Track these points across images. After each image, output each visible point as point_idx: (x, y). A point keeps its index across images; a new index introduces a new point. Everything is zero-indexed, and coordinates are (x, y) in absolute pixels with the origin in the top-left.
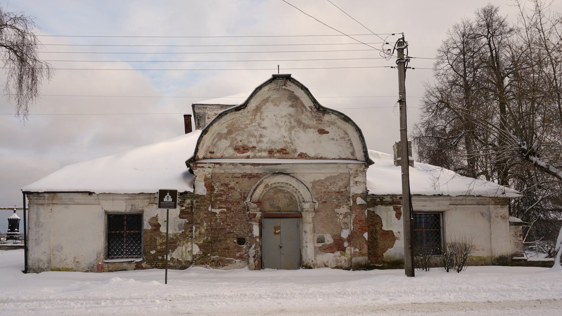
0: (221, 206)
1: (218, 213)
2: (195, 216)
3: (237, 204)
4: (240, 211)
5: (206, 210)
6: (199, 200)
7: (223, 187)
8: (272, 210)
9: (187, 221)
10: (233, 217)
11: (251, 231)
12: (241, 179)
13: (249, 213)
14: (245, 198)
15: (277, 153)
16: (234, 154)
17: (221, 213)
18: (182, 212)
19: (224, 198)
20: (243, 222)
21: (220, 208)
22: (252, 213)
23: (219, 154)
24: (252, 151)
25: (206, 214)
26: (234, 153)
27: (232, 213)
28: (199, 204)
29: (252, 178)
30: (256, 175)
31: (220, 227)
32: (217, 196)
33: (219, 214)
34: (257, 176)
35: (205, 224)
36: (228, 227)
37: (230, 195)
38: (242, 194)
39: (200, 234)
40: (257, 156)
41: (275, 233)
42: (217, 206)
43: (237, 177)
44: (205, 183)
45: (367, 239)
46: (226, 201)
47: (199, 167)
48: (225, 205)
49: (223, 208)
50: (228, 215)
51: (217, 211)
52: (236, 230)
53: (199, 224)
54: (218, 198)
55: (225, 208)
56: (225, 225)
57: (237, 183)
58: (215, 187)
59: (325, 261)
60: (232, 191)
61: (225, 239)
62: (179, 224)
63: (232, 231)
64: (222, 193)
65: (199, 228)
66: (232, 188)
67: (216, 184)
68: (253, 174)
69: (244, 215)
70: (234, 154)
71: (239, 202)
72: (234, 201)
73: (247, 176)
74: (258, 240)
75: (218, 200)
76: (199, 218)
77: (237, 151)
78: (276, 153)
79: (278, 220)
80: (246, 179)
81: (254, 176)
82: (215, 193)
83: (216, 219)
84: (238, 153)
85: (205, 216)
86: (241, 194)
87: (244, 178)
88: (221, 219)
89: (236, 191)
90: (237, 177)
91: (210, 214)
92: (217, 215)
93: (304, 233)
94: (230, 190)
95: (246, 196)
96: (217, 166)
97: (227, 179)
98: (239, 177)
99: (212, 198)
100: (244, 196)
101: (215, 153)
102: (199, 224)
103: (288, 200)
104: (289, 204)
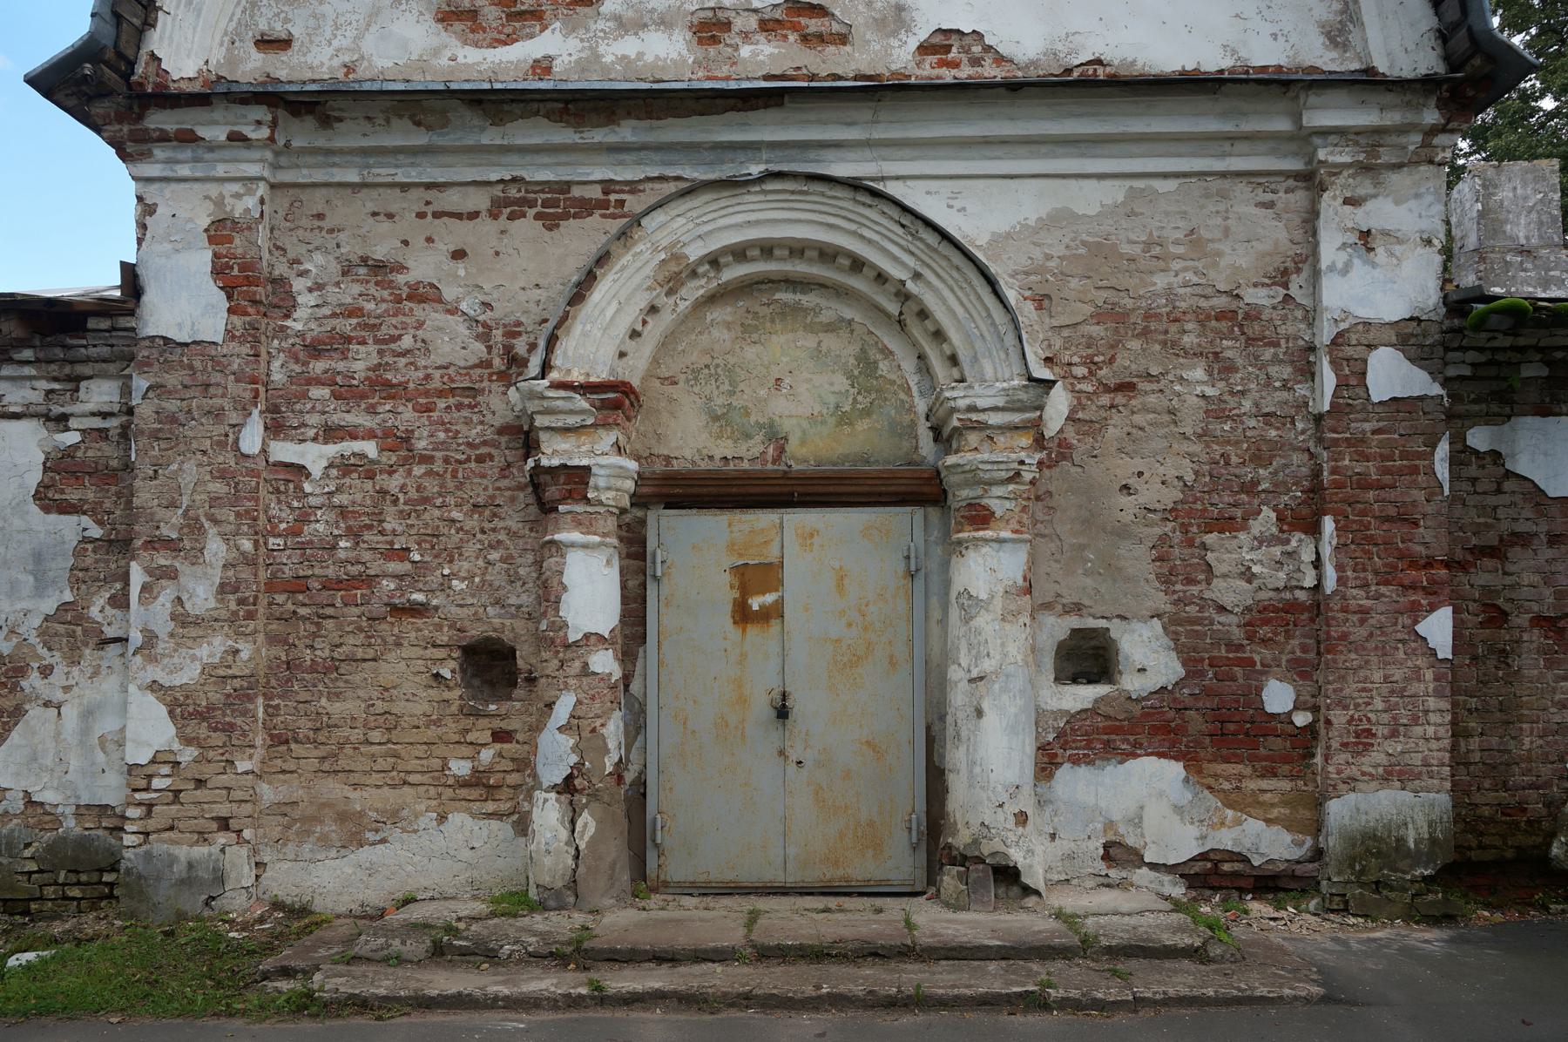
0: (336, 419)
1: (316, 470)
2: (145, 494)
3: (459, 407)
4: (480, 459)
5: (222, 445)
6: (172, 380)
7: (357, 289)
8: (724, 448)
9: (96, 532)
10: (426, 500)
11: (549, 593)
12: (486, 226)
13: (537, 466)
14: (516, 362)
15: (761, 37)
16: (436, 52)
17: (344, 466)
18: (61, 466)
19: (361, 362)
20: (502, 536)
21: (331, 433)
22: (555, 462)
23: (330, 51)
24: (570, 30)
25: (223, 475)
26: (435, 41)
27: (418, 470)
28: (172, 405)
29: (566, 216)
30: (595, 193)
31: (331, 572)
32: (315, 349)
33: (326, 475)
34: (604, 205)
35: (216, 548)
36: (394, 567)
37: (407, 342)
38: (498, 334)
39: (182, 619)
40: (608, 59)
41: (743, 615)
42: (313, 419)
43: (458, 216)
44: (216, 255)
45: (1445, 652)
46: (381, 386)
47: (164, 138)
48: (372, 411)
49: (354, 437)
50: (393, 483)
51: (315, 456)
52: (445, 585)
53: (170, 545)
54: (318, 367)
55: (370, 435)
56: (367, 556)
57: (459, 255)
58: (299, 285)
59: (1116, 817)
60: (419, 311)
61: (370, 653)
62: (38, 557)
63: (419, 597)
64: (347, 325)
65: (171, 574)
66: (424, 294)
67: (308, 266)
68: (576, 192)
69: (505, 483)
70: (436, 52)
71: (472, 391)
72: (436, 384)
73: (532, 204)
74: (604, 662)
75: (319, 382)
76: (172, 505)
77: (458, 26)
78: (746, 36)
79: (764, 519)
80: (528, 227)
81: (586, 208)
82: (299, 326)
83: (304, 518)
84: (465, 43)
85: (218, 487)
86: (485, 337)
87: (511, 217)
88: (343, 512)
89: (453, 311)
90: (458, 216)
91: (254, 473)
92: (308, 488)
93: (954, 614)
94: (407, 305)
95: (520, 346)
96: (302, 134)
97: (386, 226)
98: (473, 215)
99: (276, 365)
100: (508, 349)
101: (296, 45)
102: (170, 545)
103: (841, 382)
104: (847, 408)
